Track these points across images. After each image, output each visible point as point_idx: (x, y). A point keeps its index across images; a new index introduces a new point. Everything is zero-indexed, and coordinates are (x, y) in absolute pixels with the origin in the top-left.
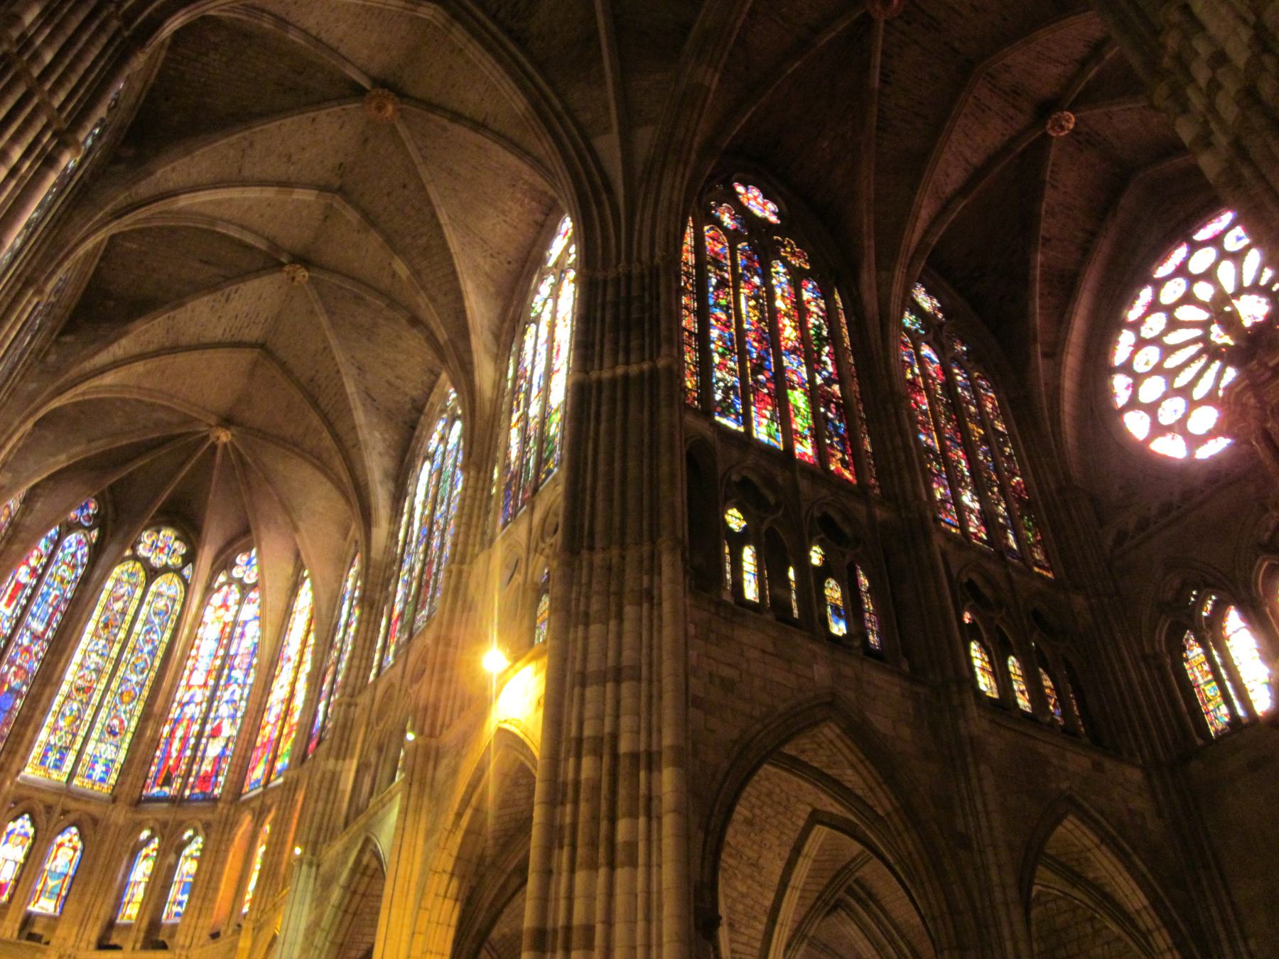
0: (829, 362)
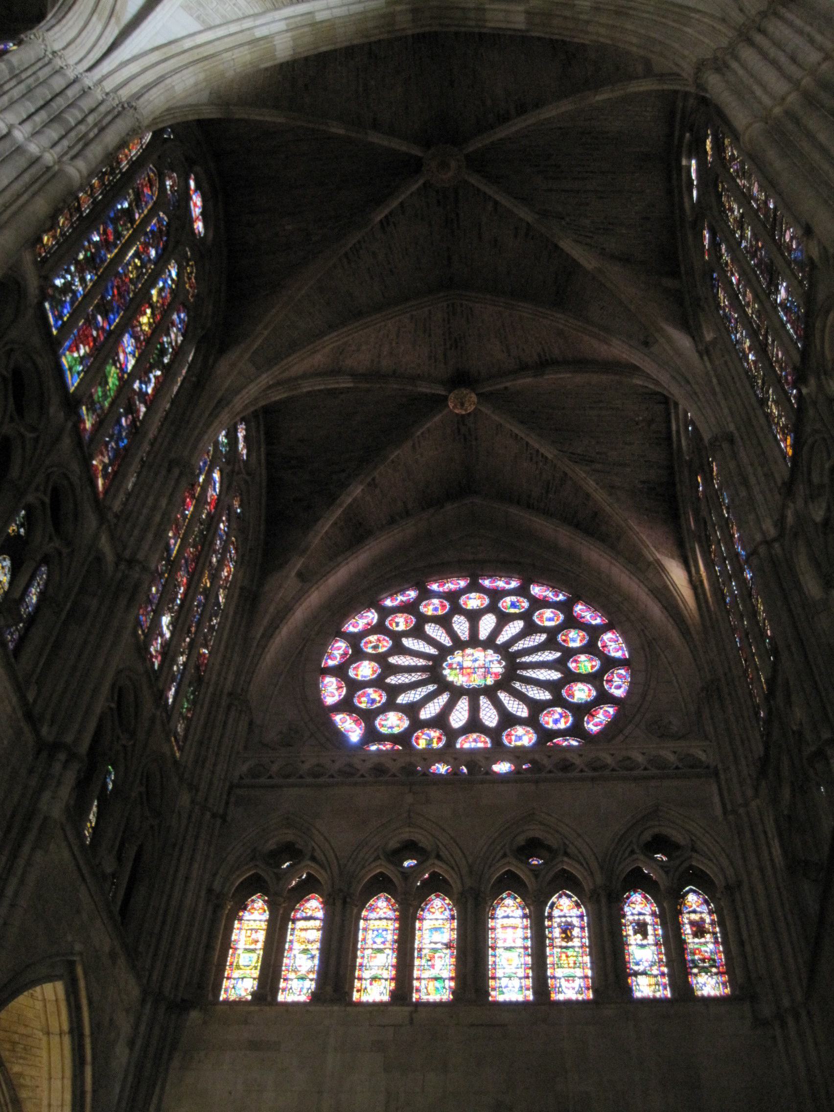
0: (152, 385)
